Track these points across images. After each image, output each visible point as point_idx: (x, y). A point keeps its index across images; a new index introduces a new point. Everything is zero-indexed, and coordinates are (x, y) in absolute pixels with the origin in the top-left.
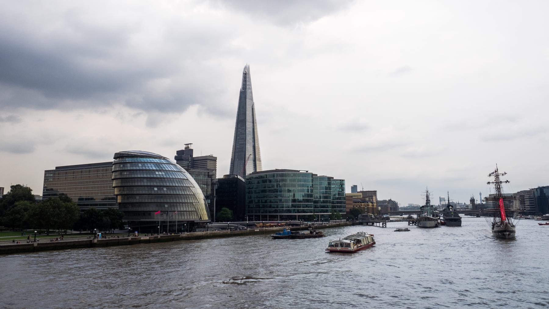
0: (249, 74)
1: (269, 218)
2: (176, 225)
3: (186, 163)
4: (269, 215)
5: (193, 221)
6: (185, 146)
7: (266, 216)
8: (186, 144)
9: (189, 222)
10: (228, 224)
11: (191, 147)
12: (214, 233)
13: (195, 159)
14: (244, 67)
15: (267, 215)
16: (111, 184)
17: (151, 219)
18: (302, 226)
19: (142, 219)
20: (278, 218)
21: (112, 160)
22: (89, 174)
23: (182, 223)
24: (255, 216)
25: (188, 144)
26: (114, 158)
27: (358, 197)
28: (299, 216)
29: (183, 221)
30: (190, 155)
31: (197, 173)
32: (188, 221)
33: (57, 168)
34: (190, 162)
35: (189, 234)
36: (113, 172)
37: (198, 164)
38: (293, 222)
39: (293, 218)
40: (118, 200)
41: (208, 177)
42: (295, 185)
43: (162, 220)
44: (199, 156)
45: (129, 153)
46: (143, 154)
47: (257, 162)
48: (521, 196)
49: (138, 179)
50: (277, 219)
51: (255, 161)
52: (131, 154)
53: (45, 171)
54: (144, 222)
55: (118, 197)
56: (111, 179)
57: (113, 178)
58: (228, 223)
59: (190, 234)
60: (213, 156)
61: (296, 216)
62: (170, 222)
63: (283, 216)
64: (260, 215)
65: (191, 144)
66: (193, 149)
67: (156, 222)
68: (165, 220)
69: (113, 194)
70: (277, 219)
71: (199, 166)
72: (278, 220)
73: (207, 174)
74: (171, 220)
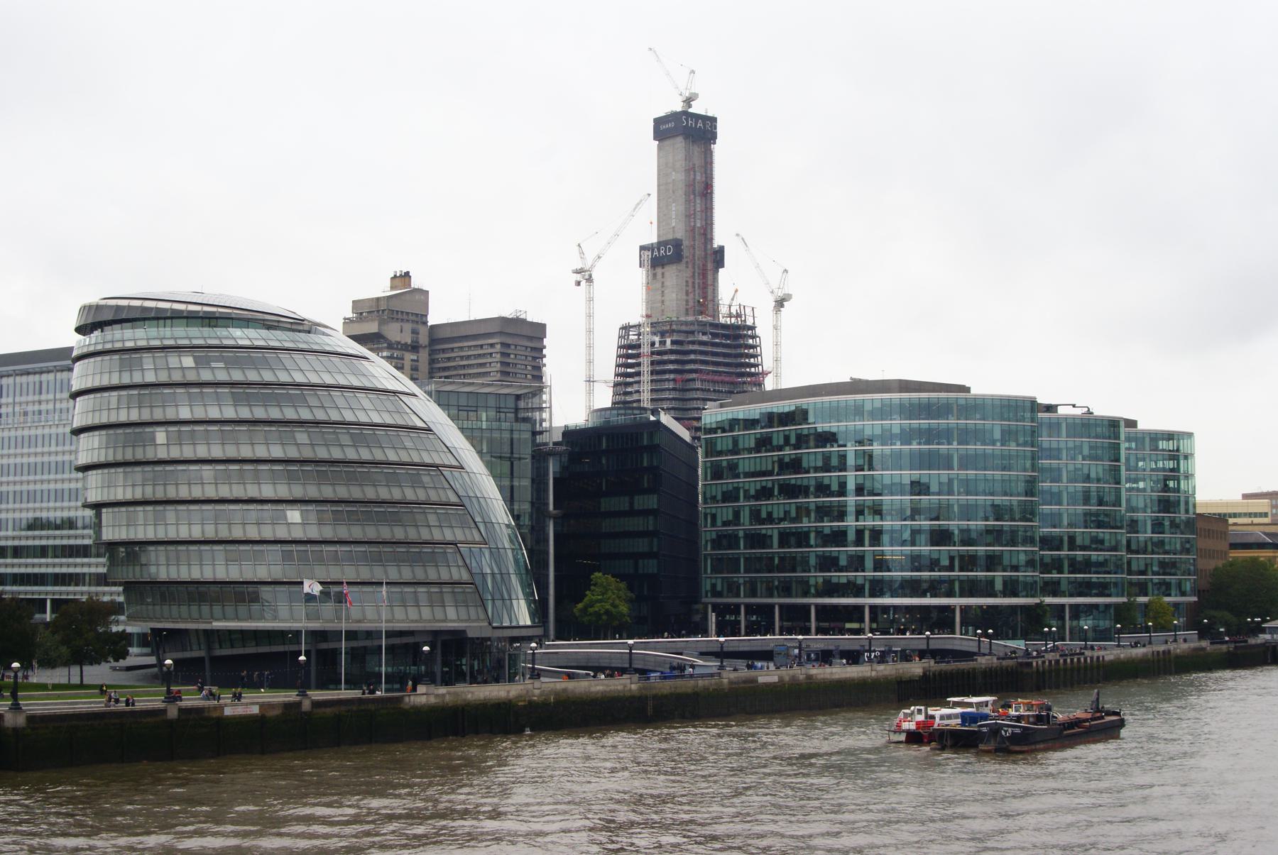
1: (817, 619)
10: (631, 647)
12: (565, 690)
15: (806, 608)
16: (71, 452)
17: (262, 618)
18: (983, 661)
19: (217, 620)
20: (861, 620)
21: (74, 341)
23: (410, 640)
24: (750, 609)
26: (80, 330)
27: (1257, 520)
28: (965, 610)
29: (411, 633)
31: (463, 402)
32: (436, 633)
35: (443, 695)
36: (75, 395)
38: (941, 640)
39: (941, 619)
40: (104, 530)
42: (949, 458)
43: (315, 625)
49: (197, 428)
50: (855, 626)
52: (157, 309)
54: (230, 632)
55: (104, 516)
56: (68, 430)
57: (75, 426)
58: (631, 642)
59: (449, 693)
60: (529, 319)
61: (949, 609)
62: (351, 635)
63: (886, 609)
64: (772, 606)
67: (290, 632)
68: (329, 626)
69: (80, 504)
70: (855, 626)
74: (354, 627)
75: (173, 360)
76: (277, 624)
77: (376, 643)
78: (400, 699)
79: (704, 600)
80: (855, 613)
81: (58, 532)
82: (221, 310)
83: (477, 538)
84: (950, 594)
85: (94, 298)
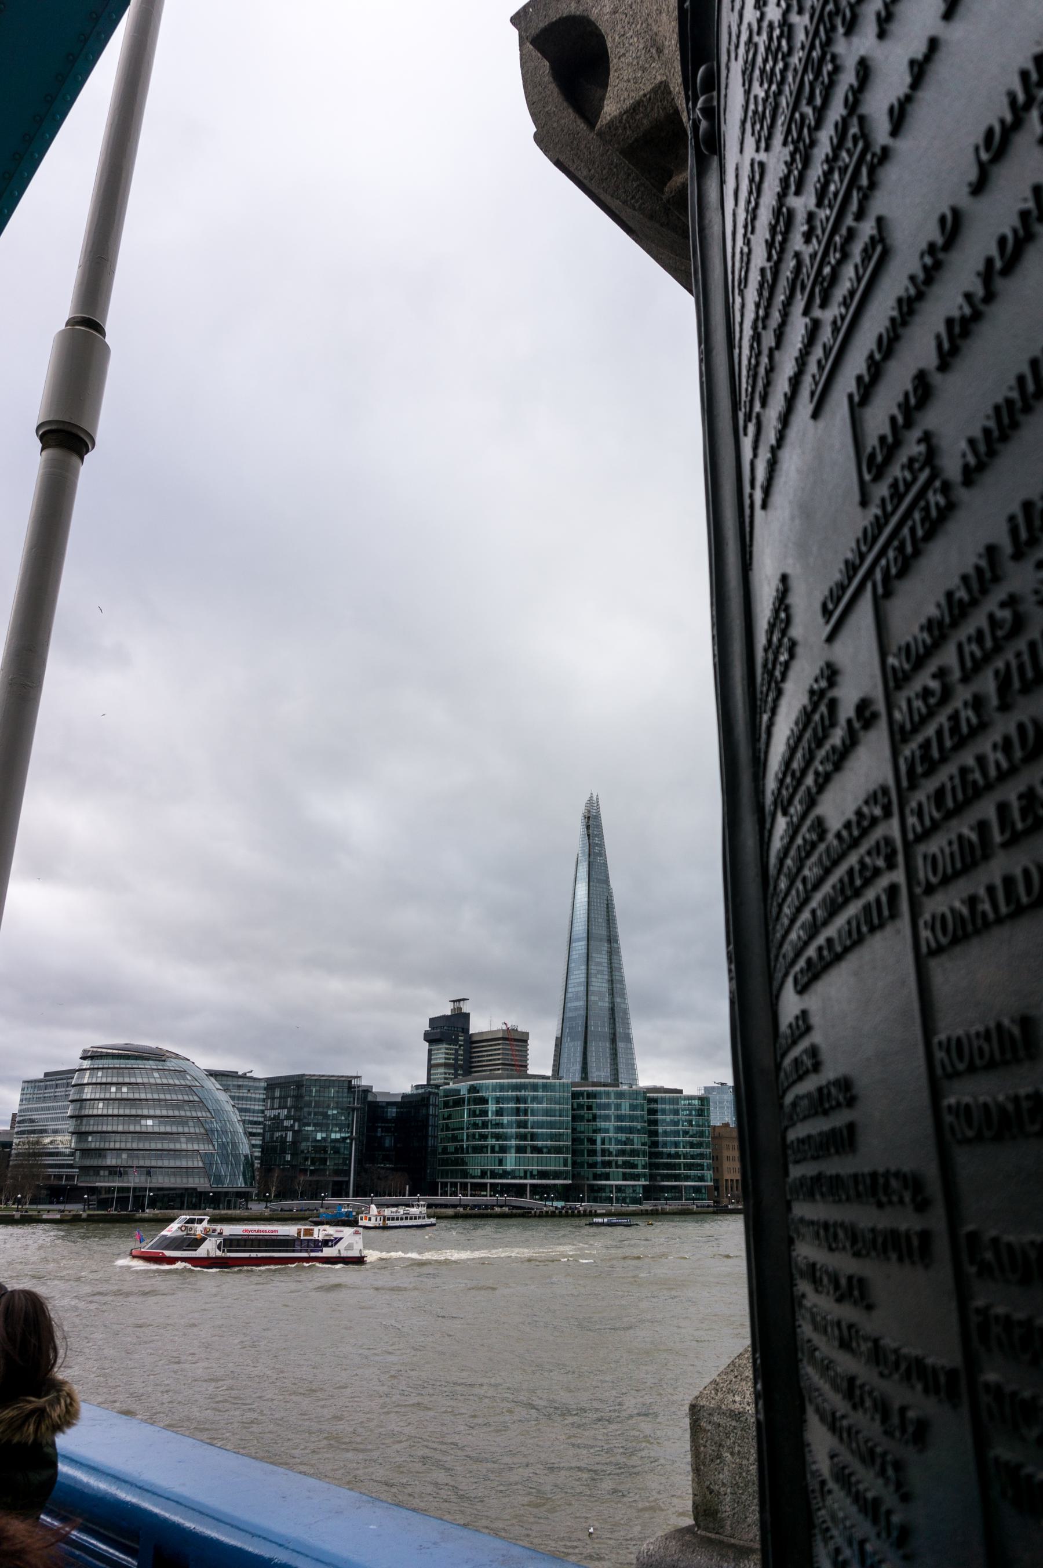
3: (451, 1049)
4: (472, 1184)
5: (195, 1189)
6: (451, 1006)
7: (444, 1185)
8: (454, 1001)
9: (190, 1191)
11: (466, 1008)
13: (475, 1039)
20: (486, 1191)
25: (459, 1001)
26: (81, 1058)
30: (463, 1029)
33: (46, 1074)
34: (460, 1046)
37: (481, 1051)
41: (348, 1092)
44: (484, 1030)
47: (621, 1045)
50: (485, 1193)
51: (613, 1040)
53: (24, 1082)
60: (519, 1030)
62: (135, 1189)
63: (497, 1184)
65: (464, 1000)
66: (469, 1014)
70: (485, 1193)
71: (484, 1056)
72: (486, 1196)
73: (346, 1084)
77: (143, 1194)
78: (134, 1215)
79: (438, 1180)
80: (483, 1186)
83: (211, 1147)
85: (88, 1047)
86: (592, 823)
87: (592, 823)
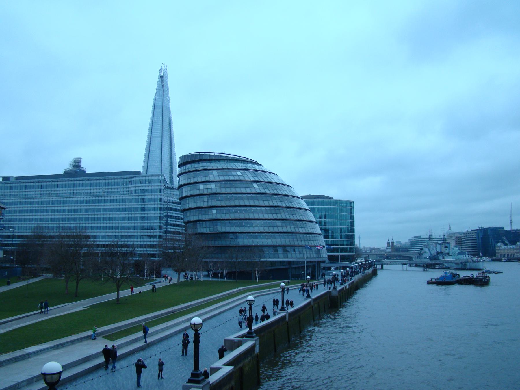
0: (167, 77)
2: (305, 266)
14: (160, 68)
22: (74, 190)
28: (341, 256)
45: (221, 155)
46: (239, 157)
48: (457, 238)
61: (338, 256)
67: (300, 262)
75: (233, 173)
76: (278, 259)
81: (148, 231)
82: (241, 158)
84: (338, 252)
86: (162, 79)
87: (162, 79)
